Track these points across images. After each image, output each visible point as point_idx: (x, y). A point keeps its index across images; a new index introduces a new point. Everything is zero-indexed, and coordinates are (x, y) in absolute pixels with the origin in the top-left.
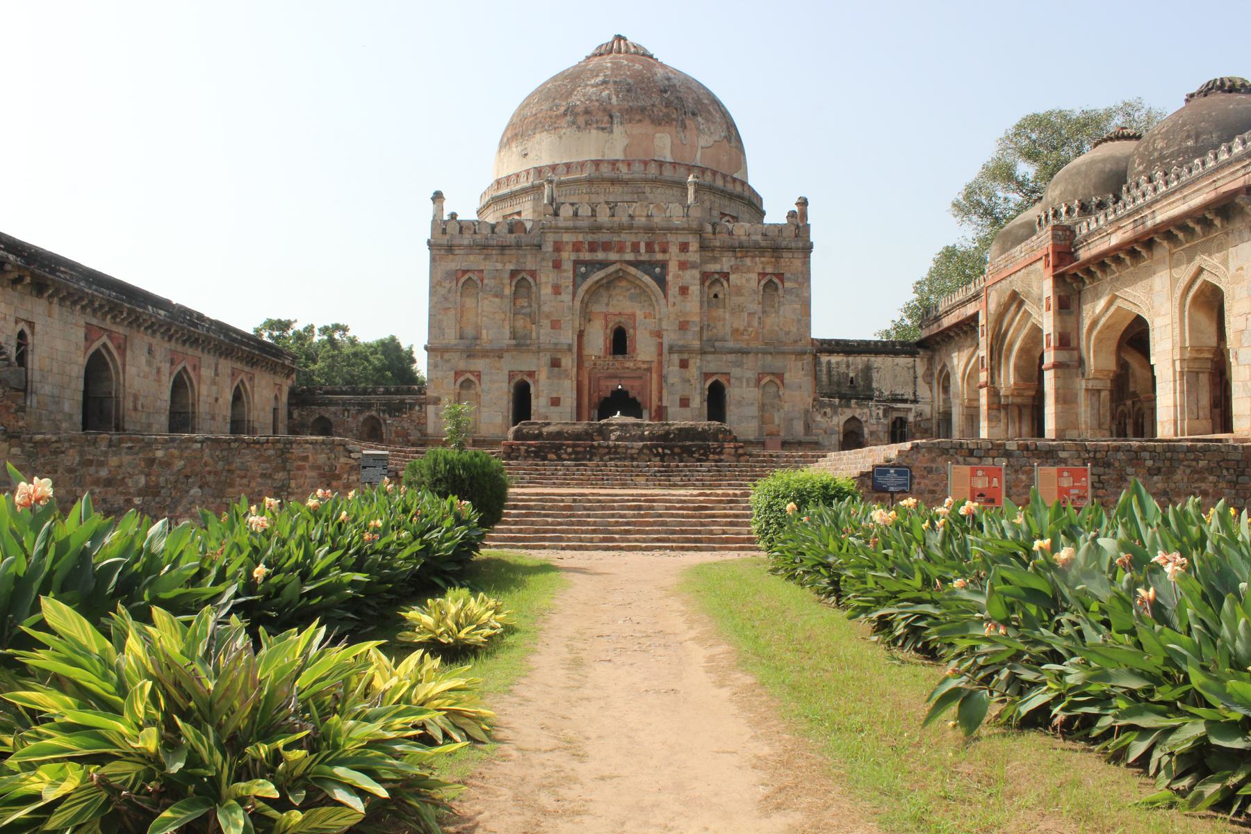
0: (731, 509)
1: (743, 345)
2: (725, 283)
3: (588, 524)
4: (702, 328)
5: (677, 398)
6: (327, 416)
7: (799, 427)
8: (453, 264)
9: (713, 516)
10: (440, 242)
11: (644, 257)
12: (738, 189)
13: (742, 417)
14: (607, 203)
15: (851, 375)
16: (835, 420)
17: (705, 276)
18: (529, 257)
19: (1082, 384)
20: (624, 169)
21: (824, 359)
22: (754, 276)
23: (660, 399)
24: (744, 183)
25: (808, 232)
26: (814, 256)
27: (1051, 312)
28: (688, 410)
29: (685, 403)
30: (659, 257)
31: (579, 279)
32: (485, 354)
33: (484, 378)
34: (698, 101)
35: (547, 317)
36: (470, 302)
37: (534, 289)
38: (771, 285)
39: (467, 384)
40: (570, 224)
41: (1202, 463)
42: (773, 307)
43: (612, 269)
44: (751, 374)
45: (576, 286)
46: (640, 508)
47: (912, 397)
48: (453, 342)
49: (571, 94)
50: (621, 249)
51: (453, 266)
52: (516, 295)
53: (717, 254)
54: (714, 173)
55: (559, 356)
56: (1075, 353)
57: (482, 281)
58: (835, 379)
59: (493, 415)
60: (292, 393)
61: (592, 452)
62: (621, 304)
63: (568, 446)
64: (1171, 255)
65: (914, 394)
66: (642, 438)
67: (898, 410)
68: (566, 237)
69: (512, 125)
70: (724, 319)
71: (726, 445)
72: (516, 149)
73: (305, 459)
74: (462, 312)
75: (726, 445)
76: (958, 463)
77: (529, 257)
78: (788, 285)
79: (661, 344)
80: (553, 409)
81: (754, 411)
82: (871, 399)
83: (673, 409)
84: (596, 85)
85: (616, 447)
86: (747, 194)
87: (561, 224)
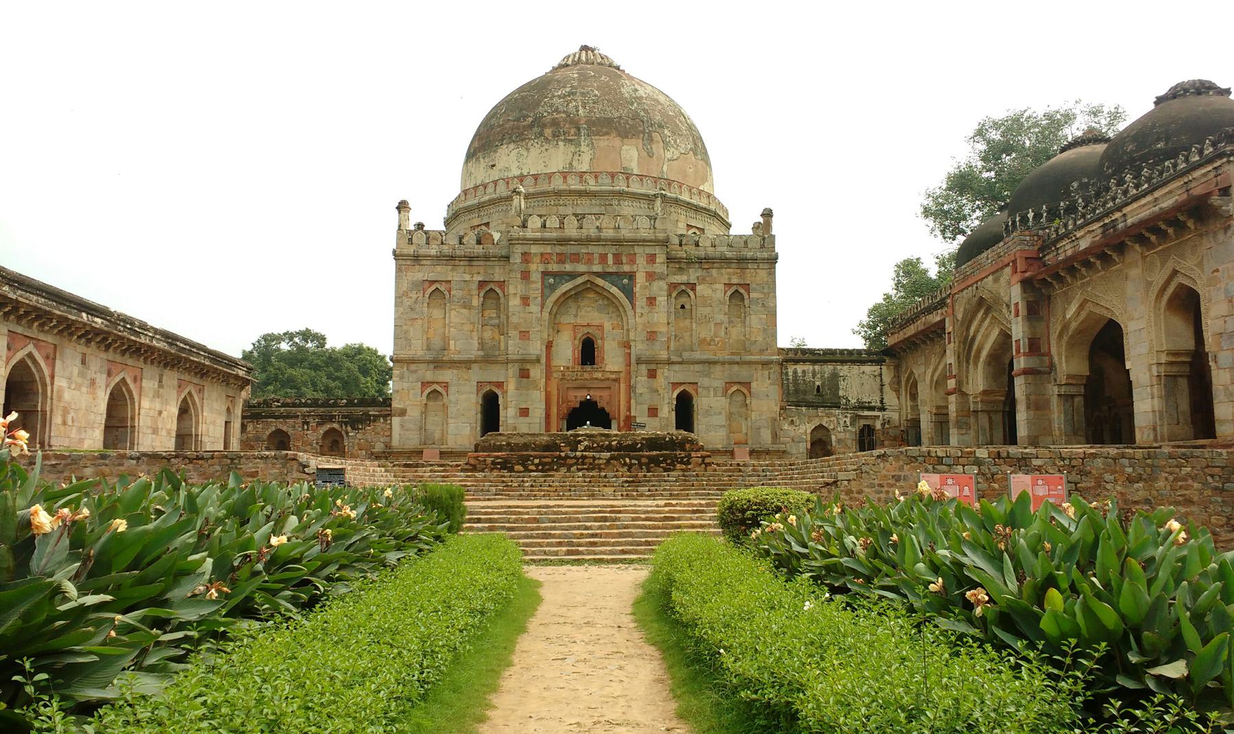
0: (697, 519)
1: (711, 357)
2: (691, 294)
3: (553, 536)
4: (669, 338)
5: (646, 407)
7: (766, 436)
8: (420, 274)
9: (679, 527)
10: (405, 252)
11: (612, 269)
12: (703, 203)
13: (710, 428)
14: (576, 215)
15: (817, 383)
16: (802, 429)
17: (673, 286)
18: (497, 269)
20: (592, 182)
22: (720, 287)
23: (629, 409)
24: (709, 196)
25: (773, 243)
26: (779, 266)
27: (1020, 318)
29: (653, 412)
30: (626, 268)
31: (547, 291)
32: (453, 364)
33: (452, 389)
34: (664, 113)
35: (516, 328)
36: (437, 313)
37: (502, 300)
38: (737, 296)
43: (580, 280)
44: (719, 384)
46: (605, 519)
47: (879, 404)
49: (538, 104)
50: (590, 262)
51: (420, 274)
53: (683, 265)
55: (528, 366)
56: (1046, 358)
57: (449, 292)
58: (802, 387)
59: (462, 428)
61: (562, 462)
62: (590, 315)
63: (535, 457)
64: (1144, 258)
65: (882, 402)
66: (609, 448)
67: (866, 417)
68: (534, 249)
69: (478, 135)
71: (693, 454)
75: (693, 454)
76: (927, 471)
77: (497, 269)
78: (753, 295)
80: (522, 419)
81: (721, 420)
84: (565, 96)
85: (584, 457)
86: (712, 207)
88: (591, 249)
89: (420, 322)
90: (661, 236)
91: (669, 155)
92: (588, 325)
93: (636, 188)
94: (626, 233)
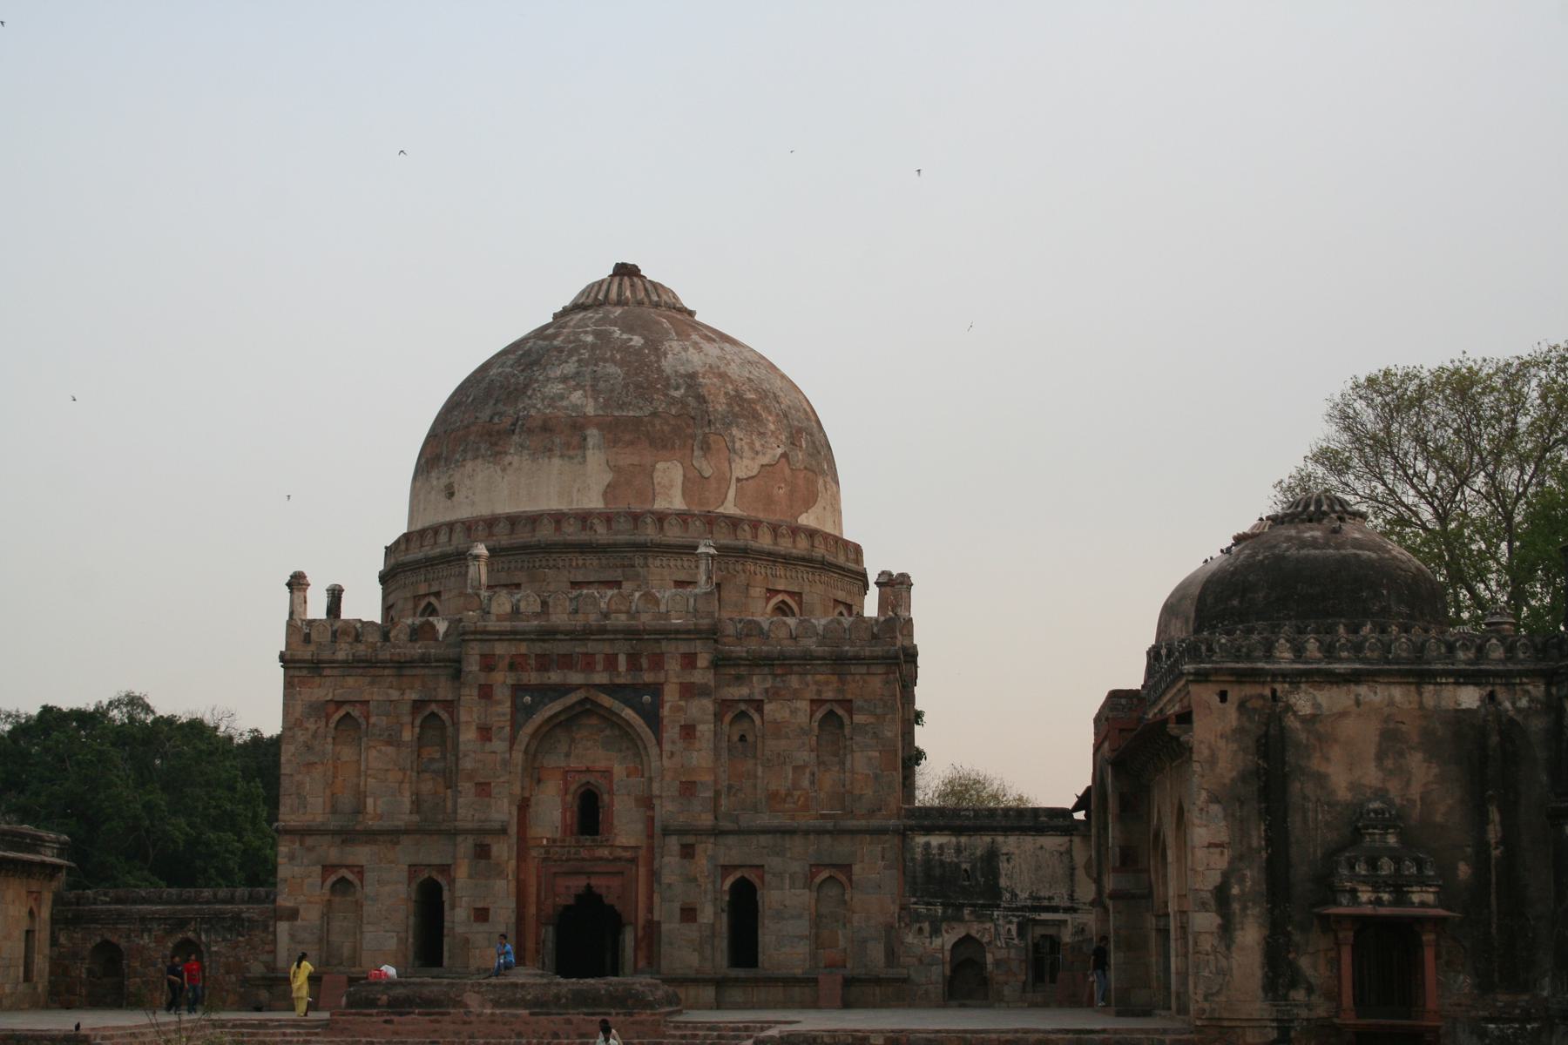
2: (756, 717)
4: (717, 793)
5: (677, 906)
6: (114, 939)
7: (876, 952)
8: (321, 691)
12: (803, 544)
13: (784, 942)
15: (964, 866)
16: (938, 942)
17: (724, 705)
19: (1151, 922)
21: (921, 840)
22: (804, 705)
23: (650, 910)
24: (812, 533)
28: (694, 926)
29: (689, 914)
30: (648, 677)
32: (371, 836)
33: (368, 876)
34: (738, 397)
36: (347, 753)
37: (450, 730)
39: (342, 886)
40: (507, 625)
42: (836, 754)
43: (573, 698)
44: (796, 867)
45: (516, 726)
47: (1068, 904)
48: (319, 819)
50: (589, 666)
51: (321, 691)
52: (420, 741)
54: (755, 525)
55: (488, 840)
57: (367, 718)
58: (938, 872)
60: (58, 900)
62: (591, 753)
67: (1044, 923)
68: (500, 649)
69: (433, 437)
70: (756, 777)
72: (438, 480)
74: (335, 767)
78: (859, 718)
79: (652, 819)
81: (803, 926)
82: (998, 906)
83: (671, 926)
84: (564, 379)
87: (493, 625)
88: (591, 647)
89: (320, 768)
90: (705, 622)
92: (588, 770)
93: (673, 534)
94: (646, 619)
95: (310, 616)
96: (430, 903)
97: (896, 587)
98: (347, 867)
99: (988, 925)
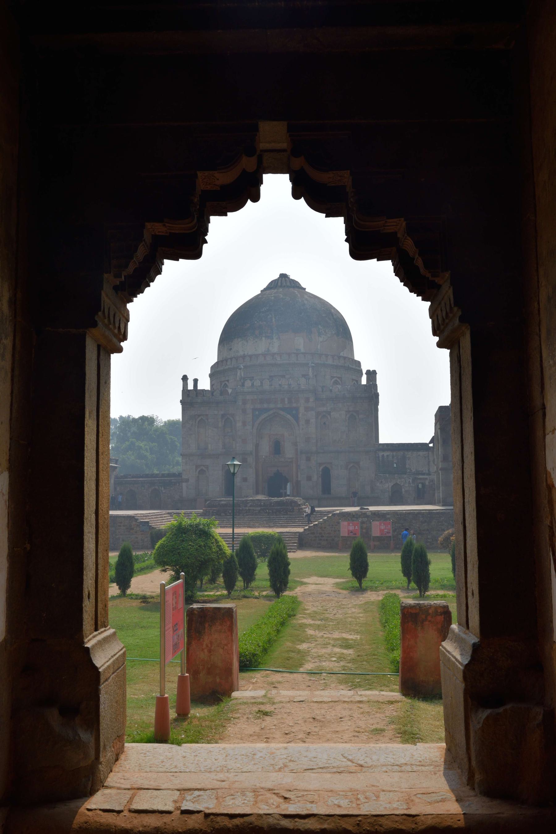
2: (329, 417)
13: (339, 486)
21: (381, 454)
23: (297, 477)
24: (345, 358)
29: (309, 478)
30: (294, 405)
39: (202, 472)
41: (442, 519)
43: (271, 412)
47: (427, 472)
54: (327, 356)
59: (214, 488)
65: (429, 470)
66: (260, 506)
67: (421, 479)
71: (295, 508)
73: (121, 523)
75: (295, 508)
85: (249, 510)
91: (321, 339)
95: (189, 389)
96: (230, 477)
97: (372, 375)
98: (204, 466)
99: (403, 480)
